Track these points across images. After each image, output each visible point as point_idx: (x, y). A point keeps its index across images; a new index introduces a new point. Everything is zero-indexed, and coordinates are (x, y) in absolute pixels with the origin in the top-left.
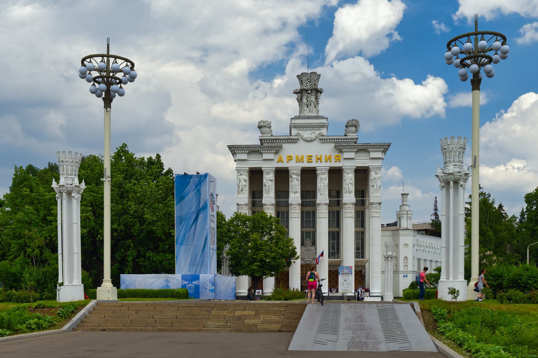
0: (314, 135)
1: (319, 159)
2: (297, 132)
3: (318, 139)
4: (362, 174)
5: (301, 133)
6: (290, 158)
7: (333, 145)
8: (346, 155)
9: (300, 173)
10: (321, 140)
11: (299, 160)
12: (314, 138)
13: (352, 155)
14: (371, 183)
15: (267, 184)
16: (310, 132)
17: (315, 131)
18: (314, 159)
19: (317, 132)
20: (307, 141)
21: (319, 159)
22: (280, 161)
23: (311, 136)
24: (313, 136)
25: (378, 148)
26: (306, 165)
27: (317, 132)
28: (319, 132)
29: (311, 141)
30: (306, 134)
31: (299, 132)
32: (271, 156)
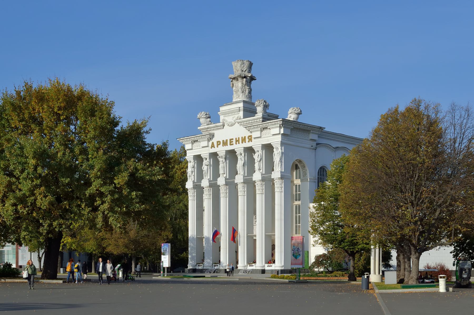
1: (237, 141)
5: (226, 118)
11: (225, 143)
19: (236, 116)
21: (237, 141)
26: (229, 148)
28: (236, 116)
29: (232, 125)
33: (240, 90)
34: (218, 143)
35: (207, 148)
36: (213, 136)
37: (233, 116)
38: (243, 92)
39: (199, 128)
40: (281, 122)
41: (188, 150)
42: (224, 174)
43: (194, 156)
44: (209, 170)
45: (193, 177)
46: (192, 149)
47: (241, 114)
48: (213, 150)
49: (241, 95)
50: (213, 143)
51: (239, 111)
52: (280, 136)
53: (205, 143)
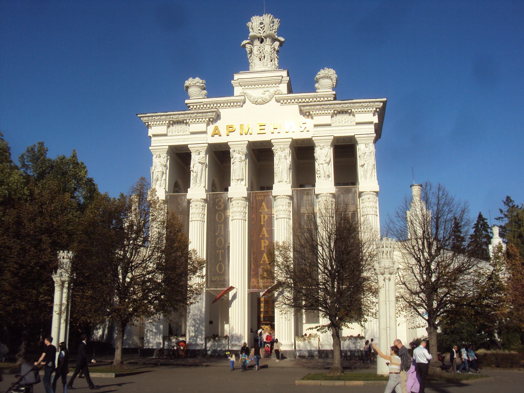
0: (267, 94)
2: (242, 91)
3: (274, 99)
4: (345, 150)
5: (249, 92)
6: (231, 129)
7: (296, 108)
8: (318, 120)
9: (245, 150)
10: (278, 101)
12: (268, 98)
13: (326, 119)
14: (359, 162)
15: (195, 169)
16: (262, 91)
17: (267, 89)
18: (269, 129)
19: (272, 90)
20: (256, 103)
22: (216, 133)
23: (262, 96)
24: (267, 96)
25: (367, 107)
27: (272, 90)
28: (275, 89)
29: (264, 102)
30: (256, 93)
31: (245, 91)
32: (202, 127)
33: (268, 57)
34: (231, 129)
35: (204, 135)
36: (218, 117)
37: (265, 89)
38: (271, 61)
39: (187, 101)
40: (381, 104)
41: (154, 136)
42: (242, 180)
43: (169, 146)
44: (204, 172)
45: (163, 182)
46: (166, 135)
47: (284, 88)
48: (217, 140)
49: (270, 64)
50: (216, 128)
51: (281, 82)
52: (373, 126)
53: (202, 127)
